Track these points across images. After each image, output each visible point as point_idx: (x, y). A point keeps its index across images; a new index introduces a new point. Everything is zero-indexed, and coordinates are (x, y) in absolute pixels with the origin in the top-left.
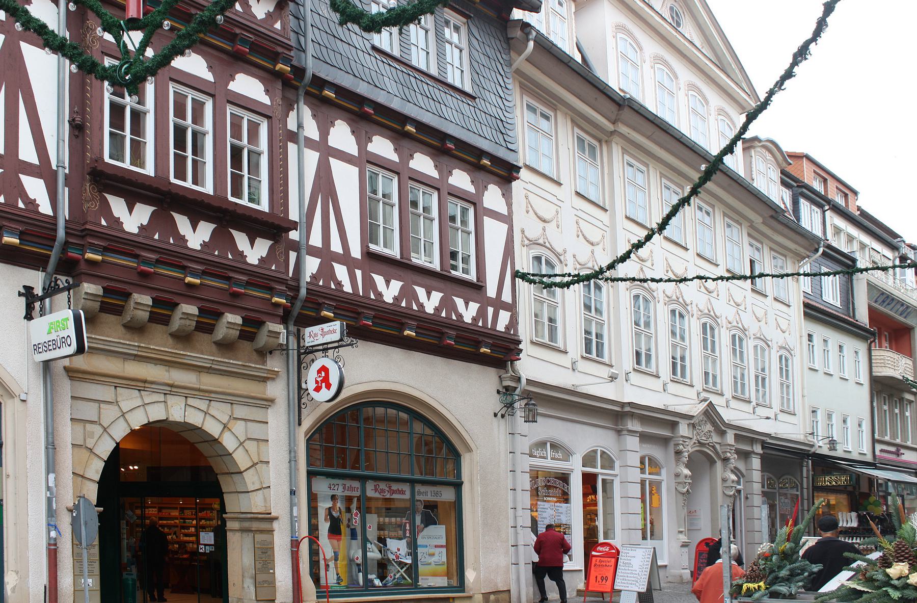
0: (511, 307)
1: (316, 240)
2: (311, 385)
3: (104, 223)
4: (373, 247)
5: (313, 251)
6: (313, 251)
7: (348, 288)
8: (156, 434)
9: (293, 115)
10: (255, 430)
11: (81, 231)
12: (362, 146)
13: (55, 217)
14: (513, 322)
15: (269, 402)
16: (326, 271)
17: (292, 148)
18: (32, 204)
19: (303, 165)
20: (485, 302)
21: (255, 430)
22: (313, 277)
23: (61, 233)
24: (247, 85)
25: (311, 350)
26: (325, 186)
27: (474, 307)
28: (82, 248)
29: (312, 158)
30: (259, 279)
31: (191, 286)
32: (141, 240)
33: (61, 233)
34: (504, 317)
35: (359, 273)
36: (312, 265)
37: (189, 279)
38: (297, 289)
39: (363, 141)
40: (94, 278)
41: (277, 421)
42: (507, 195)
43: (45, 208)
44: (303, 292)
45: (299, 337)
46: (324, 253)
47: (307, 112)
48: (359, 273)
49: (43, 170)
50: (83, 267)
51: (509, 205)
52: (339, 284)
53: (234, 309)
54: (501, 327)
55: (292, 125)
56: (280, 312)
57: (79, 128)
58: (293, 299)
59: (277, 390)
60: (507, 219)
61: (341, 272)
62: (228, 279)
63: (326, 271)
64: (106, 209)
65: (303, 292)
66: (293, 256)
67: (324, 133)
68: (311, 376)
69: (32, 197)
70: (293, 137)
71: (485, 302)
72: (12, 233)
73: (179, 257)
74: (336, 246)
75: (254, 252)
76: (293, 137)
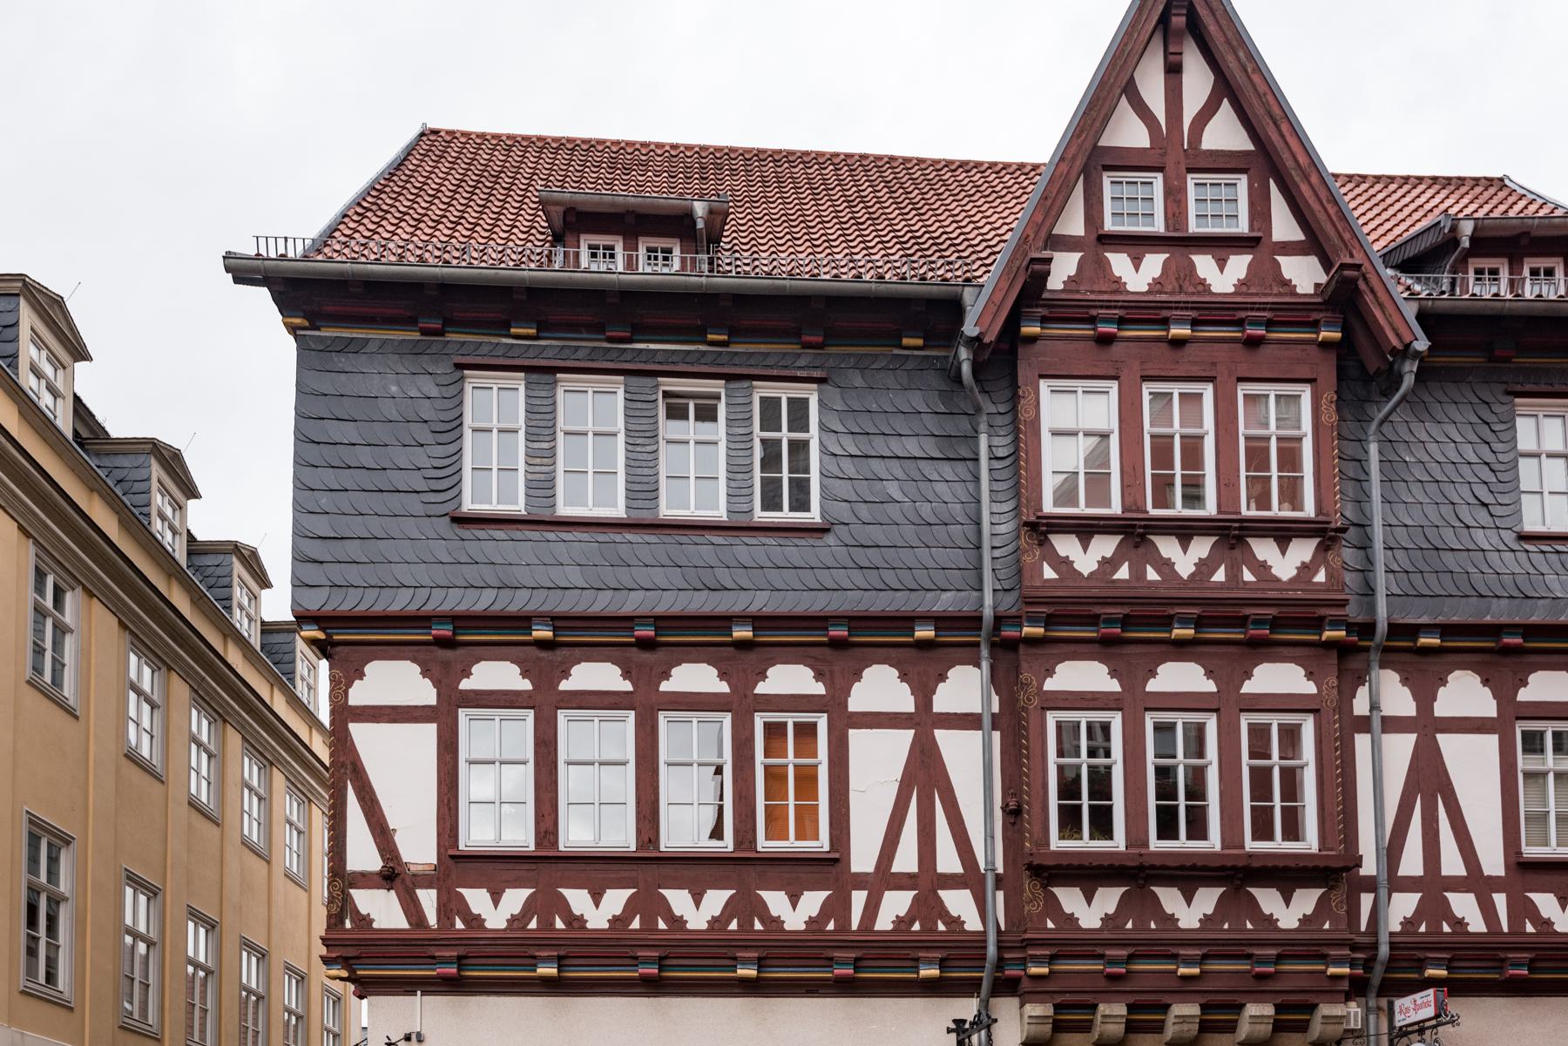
1: (1412, 863)
3: (1050, 925)
4: (1531, 851)
7: (1477, 924)
11: (1016, 943)
13: (984, 933)
22: (1407, 923)
23: (992, 950)
24: (1278, 677)
28: (1023, 962)
30: (1303, 946)
31: (1185, 978)
32: (1106, 935)
33: (992, 950)
35: (1500, 900)
37: (1182, 971)
38: (1375, 946)
43: (973, 923)
44: (1384, 950)
46: (1433, 885)
48: (1500, 900)
49: (970, 878)
50: (1025, 985)
52: (1459, 923)
53: (1259, 996)
56: (1345, 985)
57: (1017, 813)
58: (1368, 964)
61: (1464, 906)
62: (1249, 957)
64: (1054, 906)
65: (1384, 950)
66: (1367, 900)
69: (954, 913)
70: (1364, 724)
72: (930, 962)
73: (1170, 944)
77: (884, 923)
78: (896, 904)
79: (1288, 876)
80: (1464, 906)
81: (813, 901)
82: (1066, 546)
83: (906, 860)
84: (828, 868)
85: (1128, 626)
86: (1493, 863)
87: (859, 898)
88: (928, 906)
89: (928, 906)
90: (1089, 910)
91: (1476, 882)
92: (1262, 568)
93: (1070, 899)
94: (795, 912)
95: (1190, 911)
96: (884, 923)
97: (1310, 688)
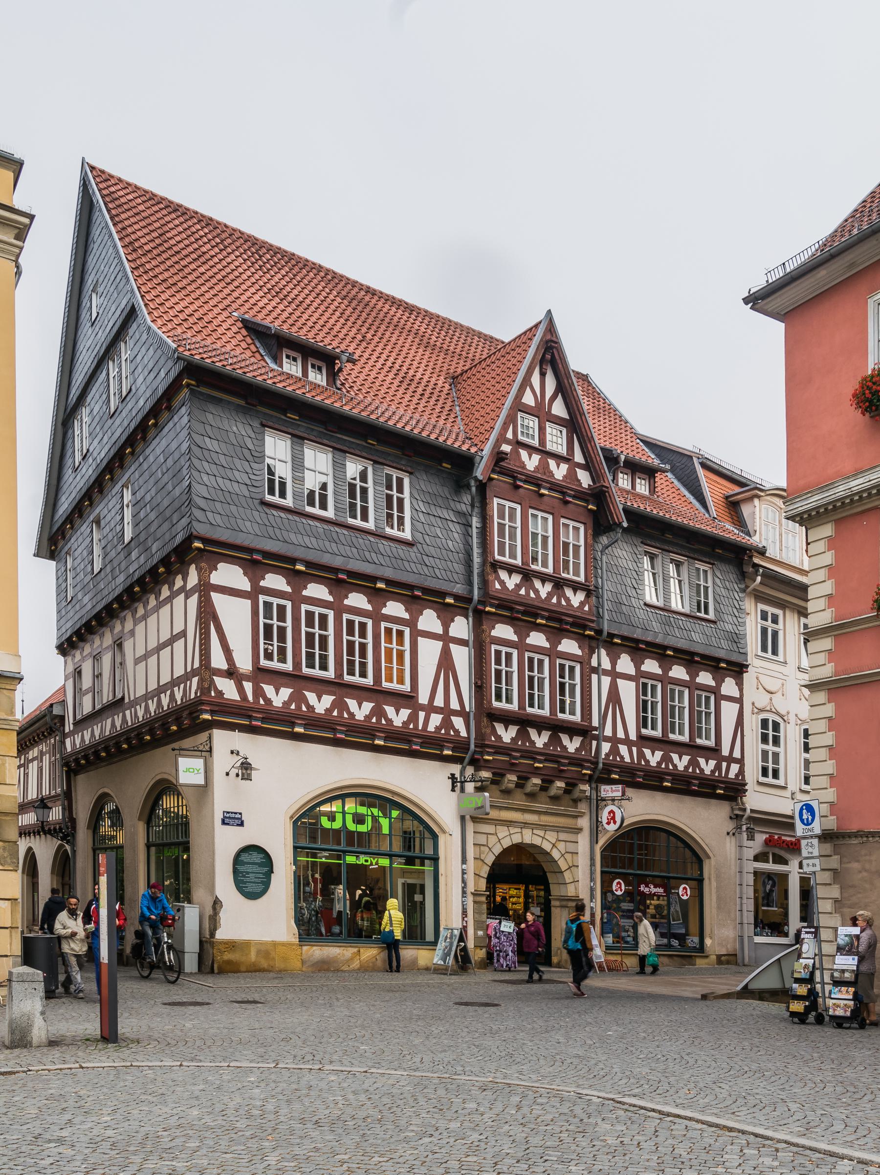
0: (741, 761)
1: (608, 732)
2: (605, 821)
5: (607, 739)
6: (607, 739)
7: (627, 759)
8: (518, 849)
9: (595, 656)
10: (571, 847)
12: (637, 667)
14: (741, 772)
15: (580, 830)
16: (614, 751)
17: (594, 677)
18: (457, 732)
19: (601, 686)
20: (720, 759)
21: (571, 847)
22: (607, 755)
25: (603, 800)
26: (614, 697)
27: (712, 763)
28: (482, 754)
29: (606, 681)
34: (735, 768)
36: (606, 747)
39: (638, 665)
40: (487, 768)
41: (583, 841)
42: (740, 685)
43: (464, 734)
44: (601, 765)
45: (597, 790)
46: (614, 740)
47: (603, 652)
49: (462, 713)
51: (741, 690)
52: (622, 757)
54: (732, 775)
55: (594, 663)
59: (584, 823)
60: (739, 701)
61: (623, 749)
63: (614, 751)
65: (601, 765)
66: (594, 743)
67: (614, 664)
68: (605, 816)
70: (595, 670)
71: (720, 759)
74: (621, 734)
75: (572, 745)
76: (595, 670)
77: (431, 728)
78: (436, 720)
79: (572, 730)
80: (623, 749)
81: (405, 713)
82: (504, 575)
83: (439, 702)
84: (407, 699)
85: (523, 615)
86: (633, 736)
87: (422, 715)
88: (447, 723)
89: (447, 723)
90: (507, 734)
91: (627, 741)
92: (568, 600)
93: (500, 729)
94: (398, 717)
95: (540, 740)
96: (431, 728)
97: (579, 652)
